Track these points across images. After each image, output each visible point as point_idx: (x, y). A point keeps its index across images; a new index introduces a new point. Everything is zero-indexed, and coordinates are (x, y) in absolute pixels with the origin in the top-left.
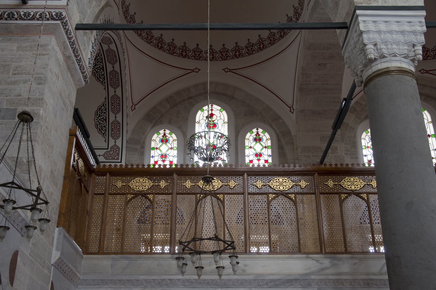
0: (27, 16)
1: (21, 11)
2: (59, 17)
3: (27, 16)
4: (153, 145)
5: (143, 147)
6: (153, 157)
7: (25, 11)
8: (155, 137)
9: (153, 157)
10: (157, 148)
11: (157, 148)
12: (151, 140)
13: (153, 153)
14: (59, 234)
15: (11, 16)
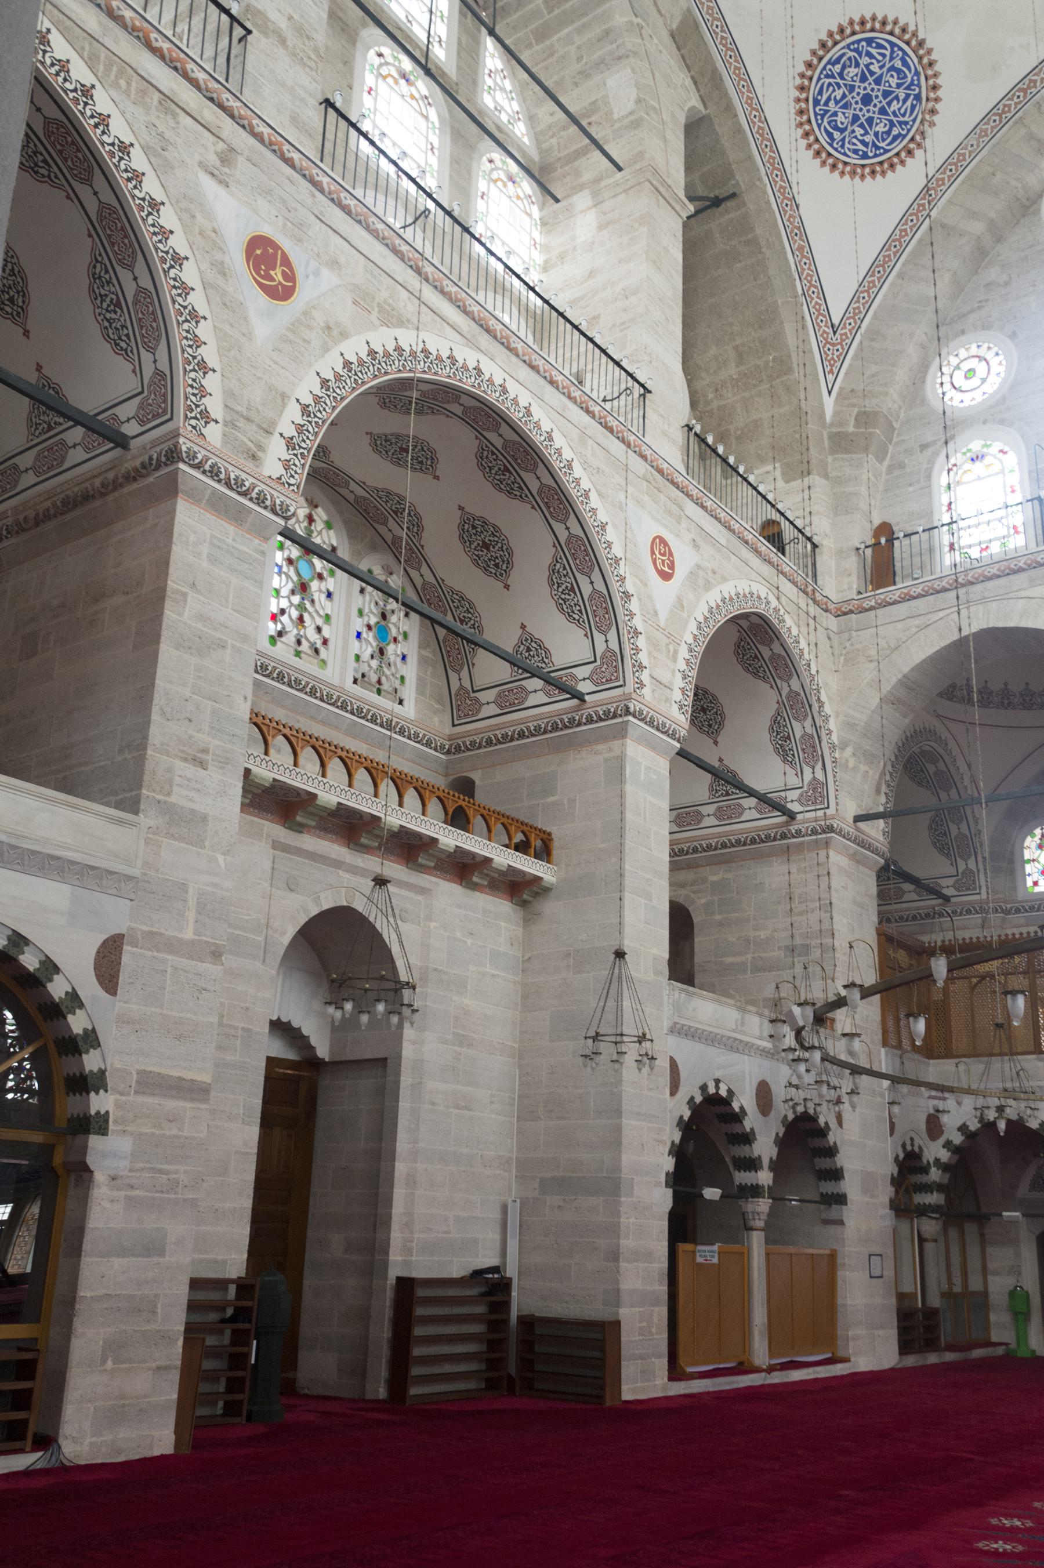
0: (799, 834)
1: (791, 828)
2: (831, 829)
3: (799, 834)
4: (1027, 855)
5: (1011, 861)
6: (1029, 875)
7: (796, 827)
8: (1028, 841)
9: (1029, 875)
10: (1034, 860)
11: (1034, 860)
12: (1022, 848)
13: (1028, 868)
14: (886, 1054)
15: (784, 836)
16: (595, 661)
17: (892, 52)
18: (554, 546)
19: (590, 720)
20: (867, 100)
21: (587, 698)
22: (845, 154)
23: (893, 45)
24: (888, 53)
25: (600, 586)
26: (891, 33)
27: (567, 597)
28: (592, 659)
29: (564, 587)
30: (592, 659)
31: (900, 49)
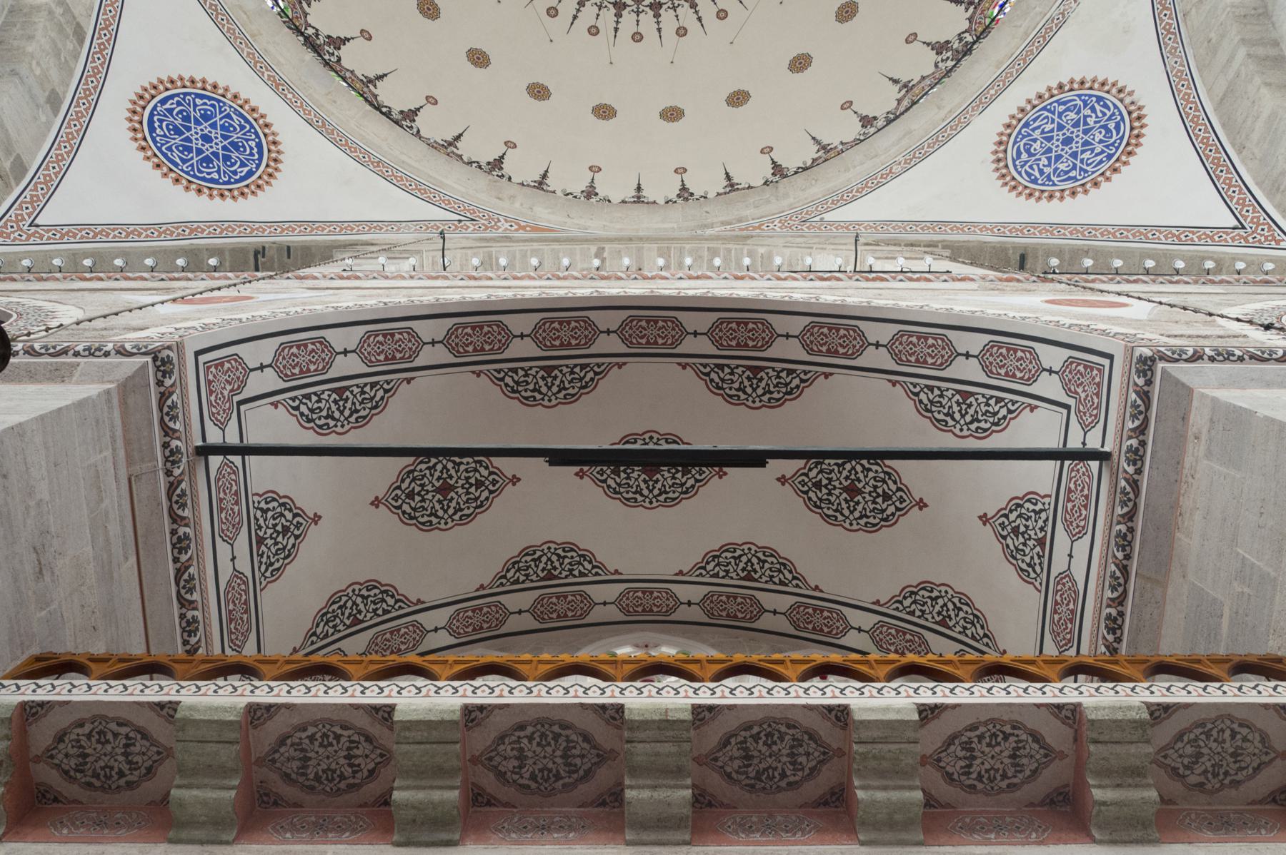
16: (1067, 407)
17: (1049, 111)
18: (894, 383)
19: (1136, 456)
20: (1067, 141)
21: (1107, 449)
22: (1093, 173)
23: (1044, 109)
24: (1046, 114)
25: (975, 343)
26: (1034, 107)
27: (971, 411)
28: (1065, 412)
29: (956, 408)
30: (1065, 412)
31: (1051, 104)
